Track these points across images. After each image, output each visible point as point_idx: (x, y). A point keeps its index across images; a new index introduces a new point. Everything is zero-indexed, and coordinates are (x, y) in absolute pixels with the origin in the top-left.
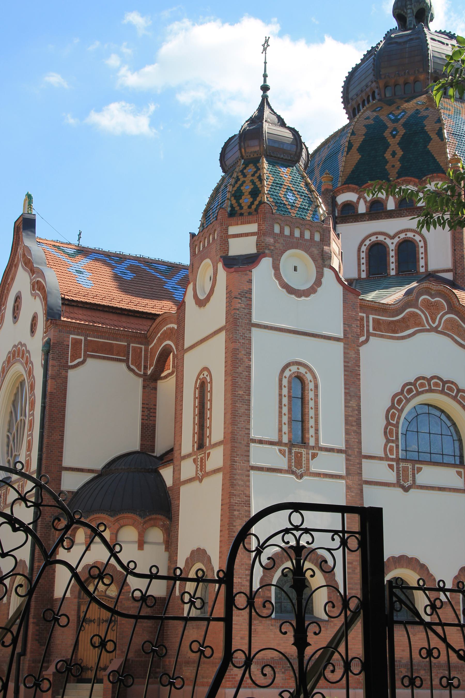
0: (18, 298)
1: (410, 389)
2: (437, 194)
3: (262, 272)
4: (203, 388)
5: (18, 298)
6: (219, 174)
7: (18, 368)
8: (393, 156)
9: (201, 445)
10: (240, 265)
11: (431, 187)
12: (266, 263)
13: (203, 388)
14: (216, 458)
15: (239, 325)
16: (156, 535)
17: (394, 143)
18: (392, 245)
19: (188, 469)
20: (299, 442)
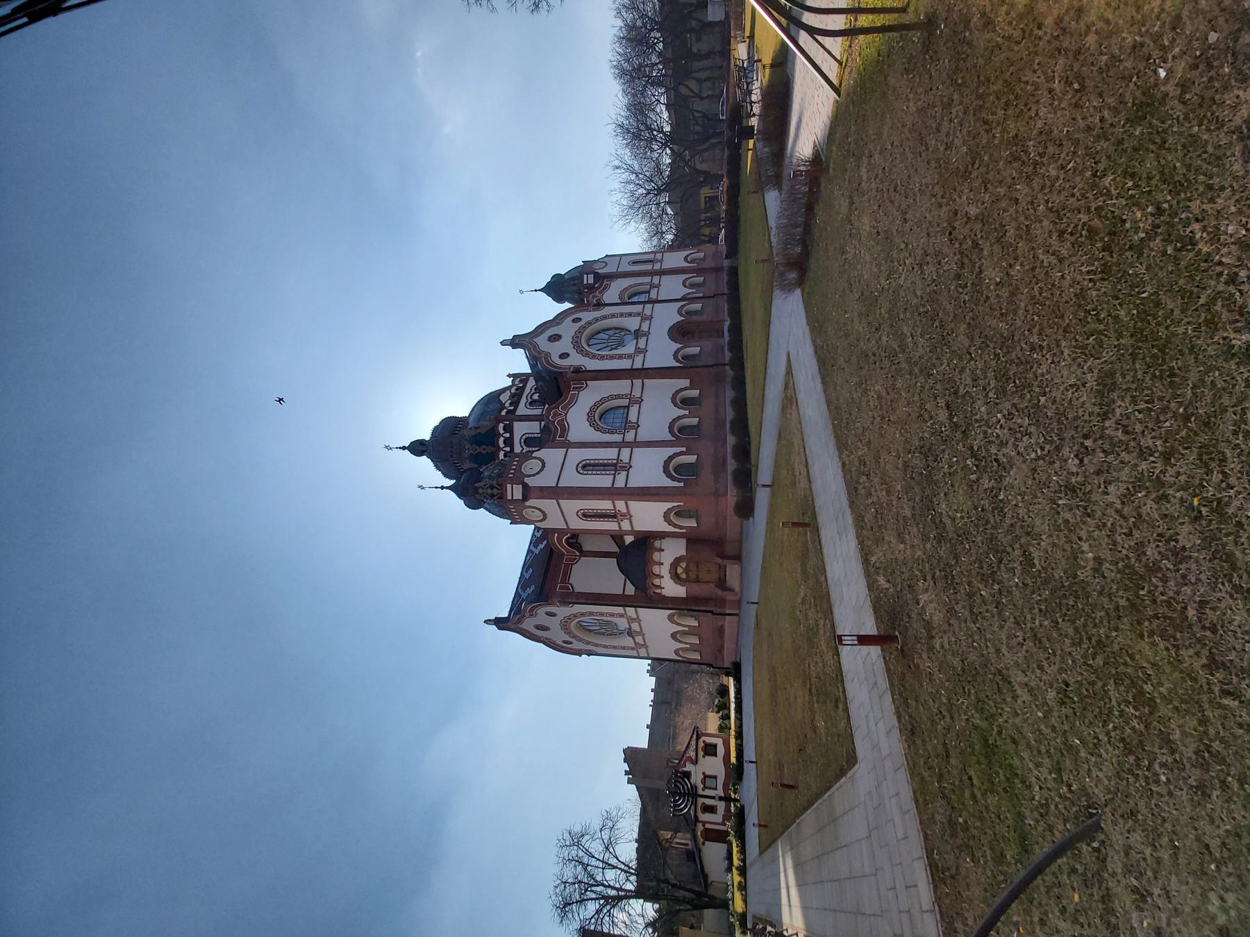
0: (538, 627)
1: (592, 423)
2: (504, 428)
3: (531, 482)
4: (586, 516)
5: (538, 627)
6: (482, 510)
7: (573, 625)
9: (615, 517)
10: (527, 492)
11: (502, 431)
12: (526, 480)
13: (586, 516)
14: (620, 505)
15: (556, 492)
16: (657, 544)
19: (626, 526)
20: (615, 467)
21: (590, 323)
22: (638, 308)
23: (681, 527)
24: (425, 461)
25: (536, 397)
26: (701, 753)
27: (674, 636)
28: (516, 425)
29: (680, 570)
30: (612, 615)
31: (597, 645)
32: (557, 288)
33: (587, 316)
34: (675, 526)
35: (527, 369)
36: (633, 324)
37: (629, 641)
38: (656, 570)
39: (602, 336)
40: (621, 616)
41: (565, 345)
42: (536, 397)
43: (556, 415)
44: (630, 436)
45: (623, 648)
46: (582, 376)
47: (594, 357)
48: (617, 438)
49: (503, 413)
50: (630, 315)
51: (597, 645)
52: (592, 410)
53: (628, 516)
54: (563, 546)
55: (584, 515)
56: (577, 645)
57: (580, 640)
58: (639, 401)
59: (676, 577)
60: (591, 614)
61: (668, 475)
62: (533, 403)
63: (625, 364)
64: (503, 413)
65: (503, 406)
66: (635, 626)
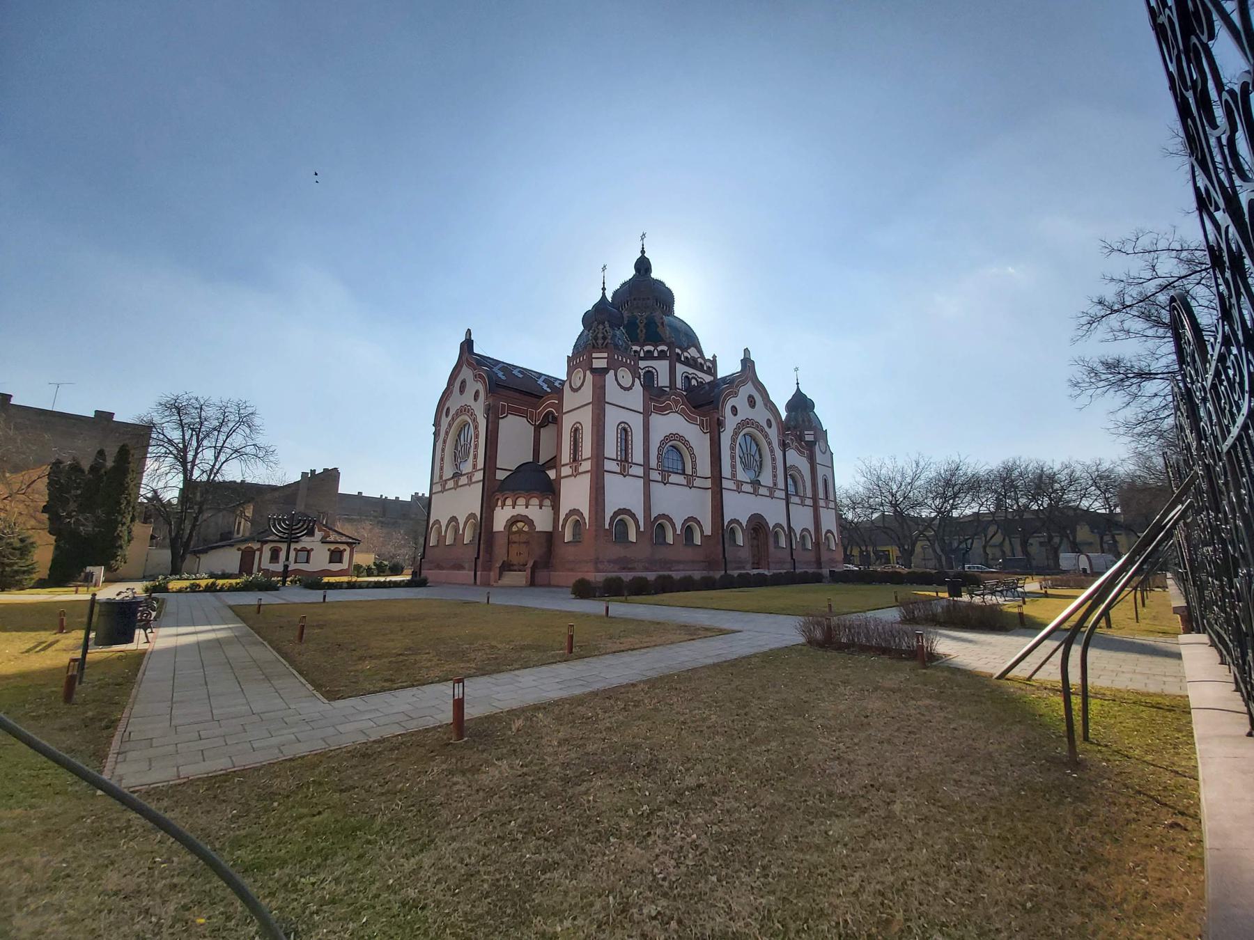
0: (463, 382)
1: (667, 438)
2: (662, 351)
4: (576, 431)
5: (463, 382)
8: (642, 333)
9: (575, 460)
11: (660, 348)
12: (612, 372)
13: (576, 431)
14: (586, 466)
15: (599, 402)
16: (547, 502)
17: (642, 326)
18: (642, 372)
19: (566, 471)
20: (625, 461)
21: (766, 436)
22: (781, 485)
23: (564, 526)
24: (630, 273)
25: (694, 382)
26: (333, 547)
27: (454, 519)
28: (666, 363)
29: (520, 525)
30: (475, 457)
31: (445, 442)
32: (801, 404)
33: (773, 433)
34: (566, 520)
35: (721, 373)
36: (766, 479)
37: (448, 473)
38: (521, 501)
39: (754, 447)
40: (475, 466)
41: (745, 412)
42: (694, 382)
43: (677, 402)
44: (655, 475)
45: (442, 468)
46: (714, 429)
47: (734, 440)
48: (653, 463)
49: (678, 351)
50: (775, 476)
51: (445, 442)
52: (680, 438)
53: (576, 473)
54: (548, 406)
55: (576, 430)
56: (445, 421)
57: (450, 425)
58: (690, 485)
59: (513, 521)
60: (477, 437)
61: (616, 514)
62: (687, 379)
63: (726, 471)
64: (678, 351)
65: (684, 350)
66: (463, 480)
